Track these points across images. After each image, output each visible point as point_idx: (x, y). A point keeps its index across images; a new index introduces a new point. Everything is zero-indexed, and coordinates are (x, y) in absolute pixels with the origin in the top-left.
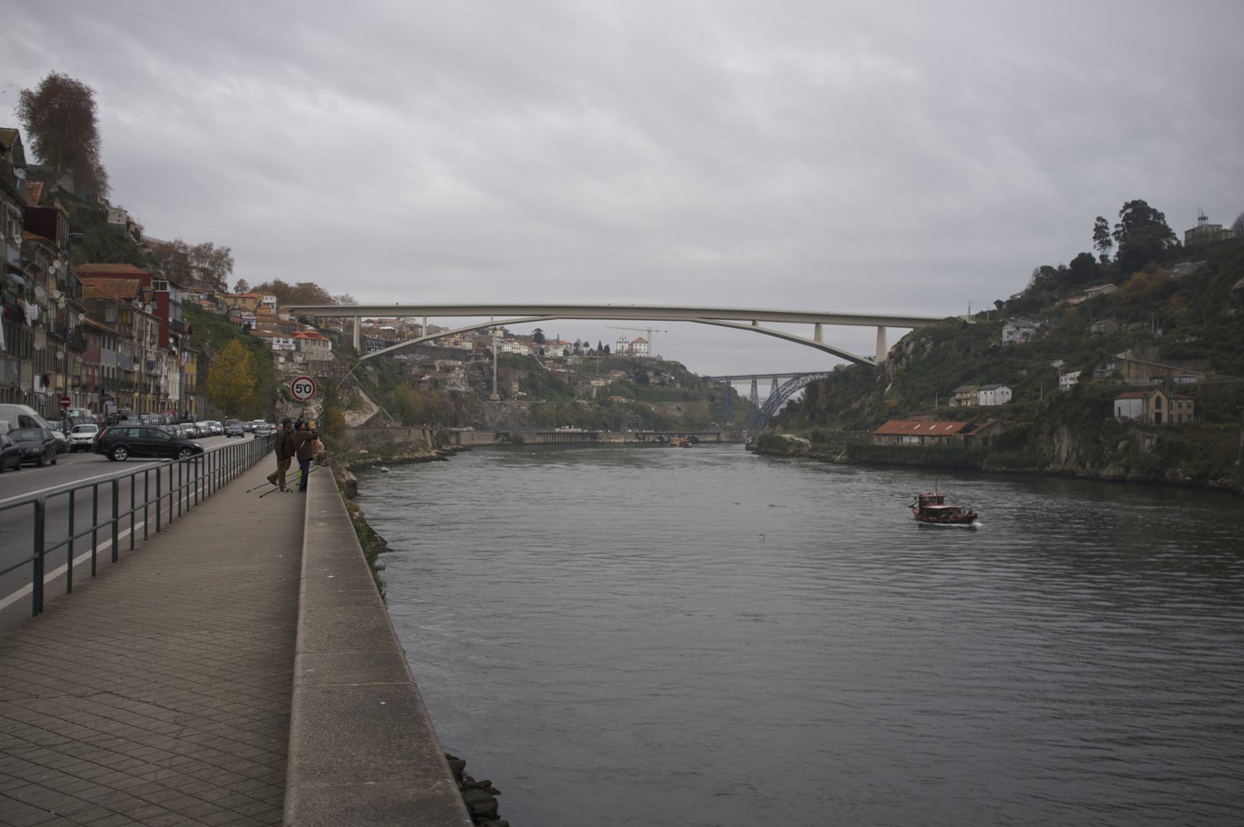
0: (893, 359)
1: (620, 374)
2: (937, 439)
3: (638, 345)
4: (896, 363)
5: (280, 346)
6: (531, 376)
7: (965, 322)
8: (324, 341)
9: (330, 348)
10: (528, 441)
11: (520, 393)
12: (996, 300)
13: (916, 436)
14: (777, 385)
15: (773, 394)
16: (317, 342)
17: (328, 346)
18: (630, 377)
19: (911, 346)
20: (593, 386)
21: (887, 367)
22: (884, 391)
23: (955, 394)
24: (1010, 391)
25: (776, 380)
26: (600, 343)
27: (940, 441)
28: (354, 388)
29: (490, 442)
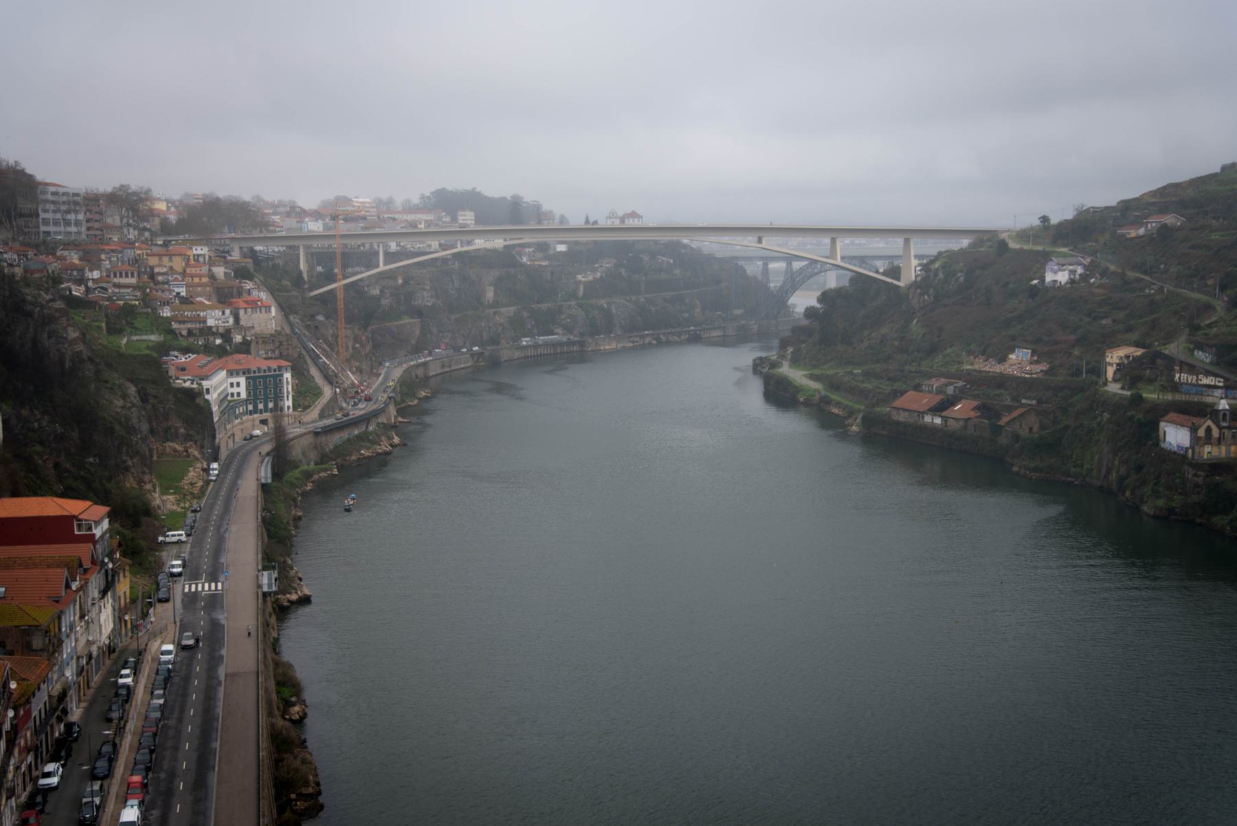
1: (608, 264)
3: (631, 220)
7: (1003, 245)
12: (1042, 215)
15: (787, 279)
19: (941, 275)
20: (580, 281)
25: (791, 263)
29: (462, 366)
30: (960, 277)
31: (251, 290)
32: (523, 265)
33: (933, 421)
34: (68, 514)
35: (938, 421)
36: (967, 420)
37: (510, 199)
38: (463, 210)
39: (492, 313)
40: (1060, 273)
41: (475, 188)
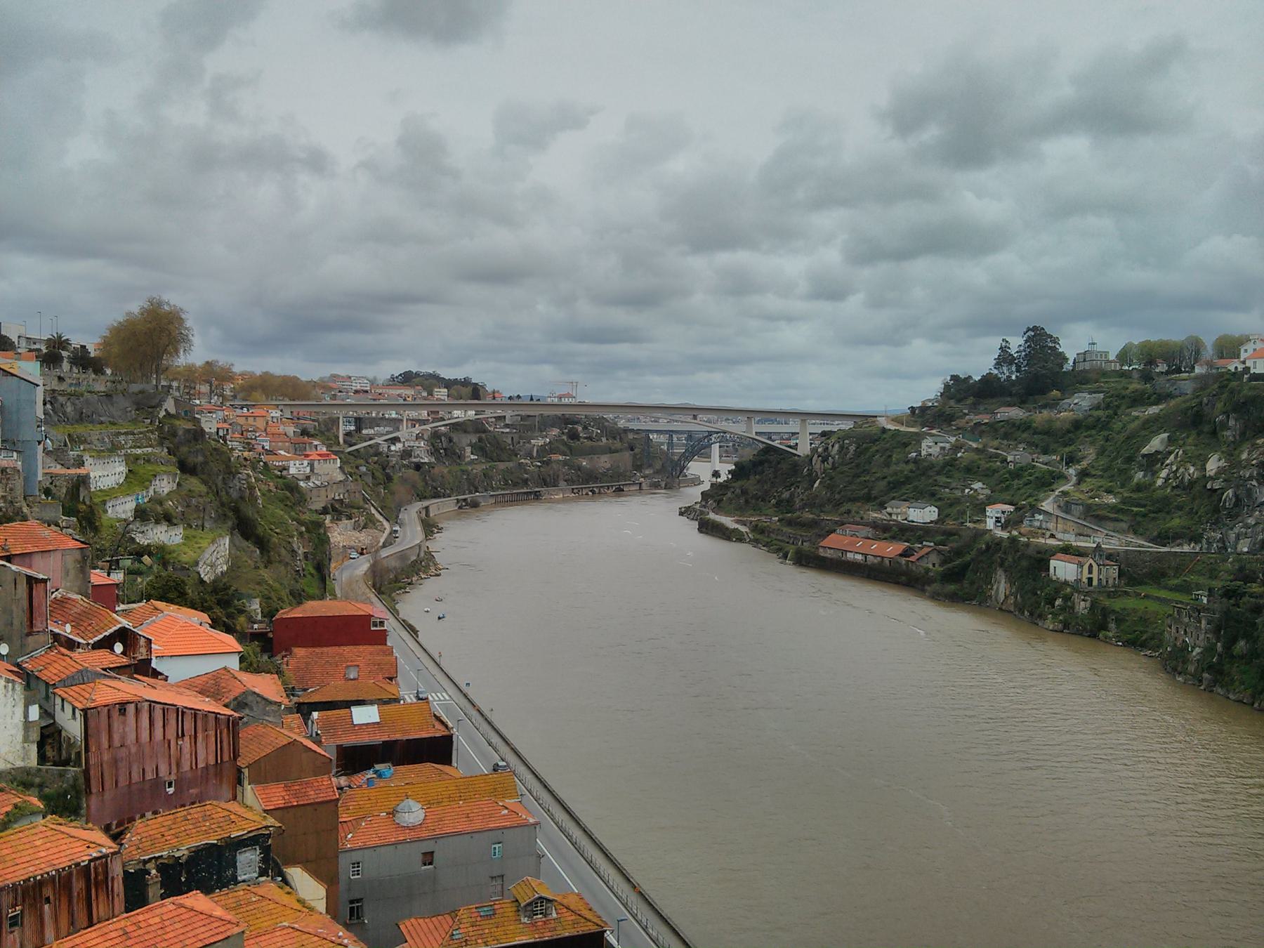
0: (820, 458)
3: (566, 399)
4: (823, 462)
5: (297, 468)
6: (480, 440)
8: (334, 459)
10: (483, 504)
11: (472, 457)
13: (860, 553)
16: (328, 461)
17: (337, 463)
18: (563, 433)
19: (837, 446)
22: (813, 486)
23: (886, 508)
24: (936, 510)
26: (532, 396)
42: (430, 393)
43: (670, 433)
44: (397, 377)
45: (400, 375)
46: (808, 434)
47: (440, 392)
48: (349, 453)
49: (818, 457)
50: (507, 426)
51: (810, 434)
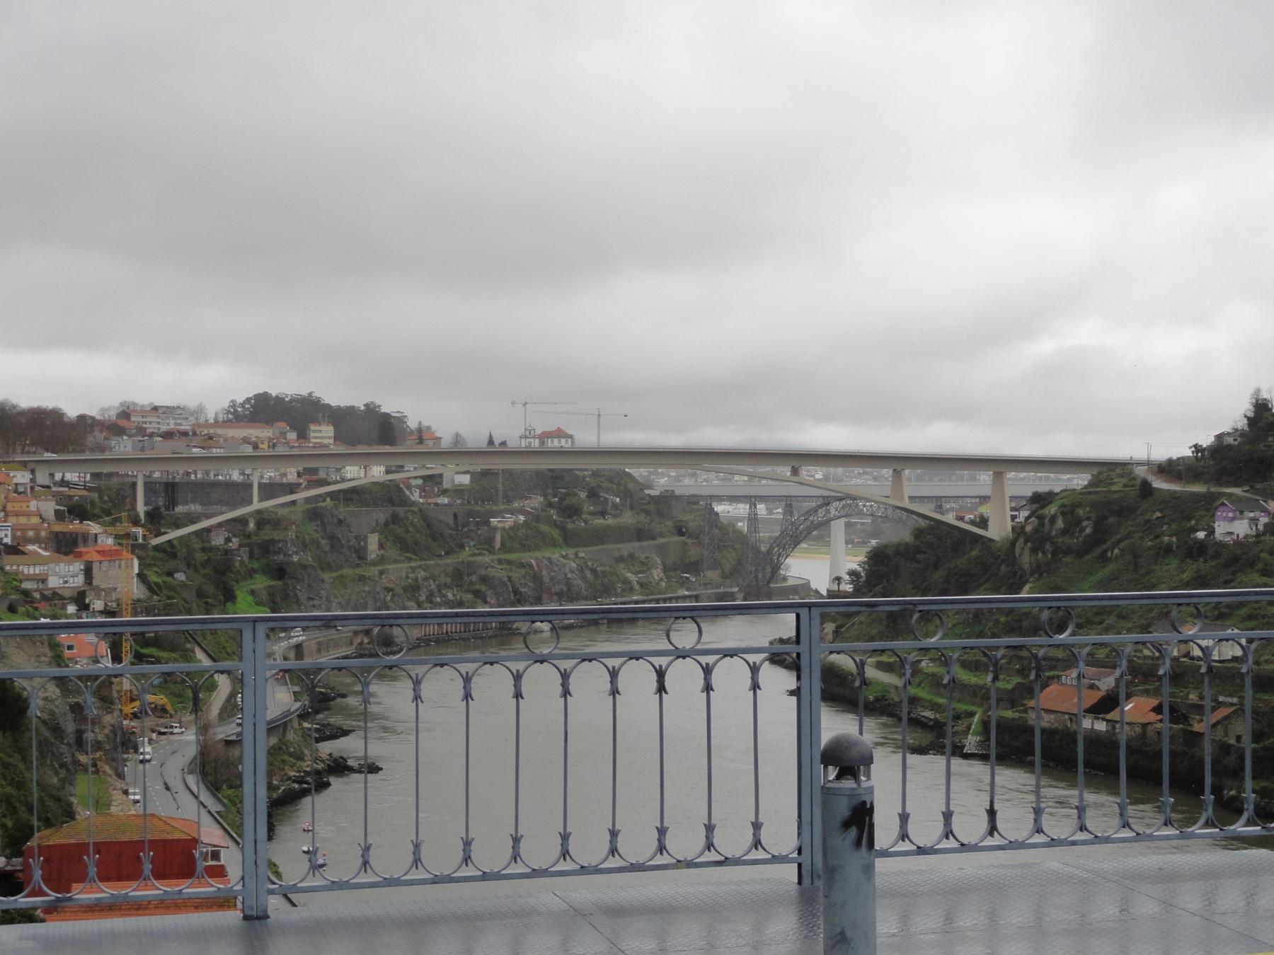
0: (1029, 544)
1: (536, 501)
2: (1138, 730)
3: (556, 440)
4: (1034, 551)
9: (136, 570)
14: (791, 514)
16: (117, 563)
18: (551, 505)
19: (1060, 523)
20: (496, 529)
21: (1020, 555)
26: (491, 436)
27: (1144, 733)
28: (188, 646)
30: (1086, 527)
31: (99, 536)
32: (414, 504)
33: (1093, 726)
34: (184, 837)
35: (1101, 726)
36: (1144, 726)
37: (362, 408)
38: (317, 422)
39: (377, 573)
40: (1236, 522)
41: (311, 393)
42: (303, 435)
43: (752, 500)
44: (242, 405)
45: (248, 400)
46: (1007, 500)
47: (321, 431)
48: (156, 548)
49: (1026, 542)
50: (444, 492)
51: (1012, 498)
